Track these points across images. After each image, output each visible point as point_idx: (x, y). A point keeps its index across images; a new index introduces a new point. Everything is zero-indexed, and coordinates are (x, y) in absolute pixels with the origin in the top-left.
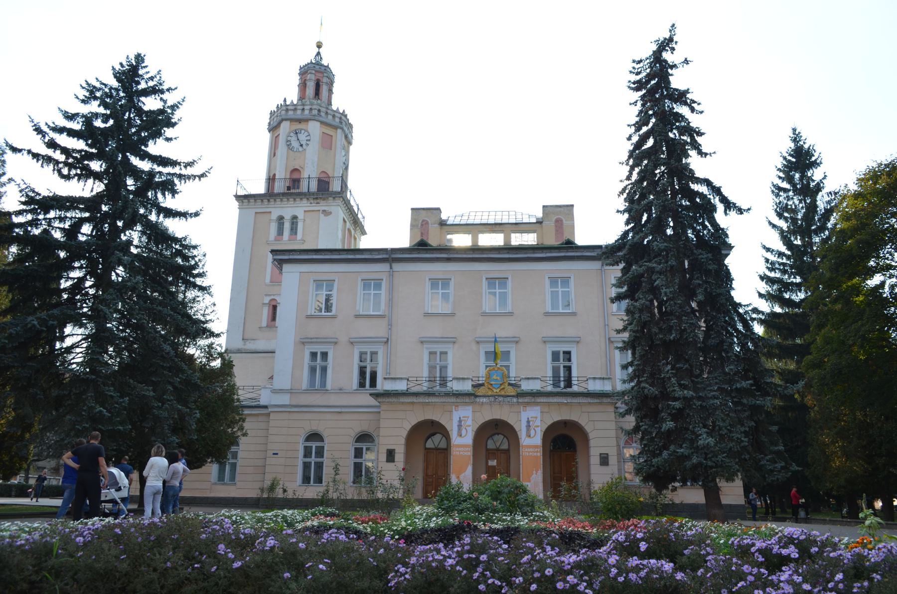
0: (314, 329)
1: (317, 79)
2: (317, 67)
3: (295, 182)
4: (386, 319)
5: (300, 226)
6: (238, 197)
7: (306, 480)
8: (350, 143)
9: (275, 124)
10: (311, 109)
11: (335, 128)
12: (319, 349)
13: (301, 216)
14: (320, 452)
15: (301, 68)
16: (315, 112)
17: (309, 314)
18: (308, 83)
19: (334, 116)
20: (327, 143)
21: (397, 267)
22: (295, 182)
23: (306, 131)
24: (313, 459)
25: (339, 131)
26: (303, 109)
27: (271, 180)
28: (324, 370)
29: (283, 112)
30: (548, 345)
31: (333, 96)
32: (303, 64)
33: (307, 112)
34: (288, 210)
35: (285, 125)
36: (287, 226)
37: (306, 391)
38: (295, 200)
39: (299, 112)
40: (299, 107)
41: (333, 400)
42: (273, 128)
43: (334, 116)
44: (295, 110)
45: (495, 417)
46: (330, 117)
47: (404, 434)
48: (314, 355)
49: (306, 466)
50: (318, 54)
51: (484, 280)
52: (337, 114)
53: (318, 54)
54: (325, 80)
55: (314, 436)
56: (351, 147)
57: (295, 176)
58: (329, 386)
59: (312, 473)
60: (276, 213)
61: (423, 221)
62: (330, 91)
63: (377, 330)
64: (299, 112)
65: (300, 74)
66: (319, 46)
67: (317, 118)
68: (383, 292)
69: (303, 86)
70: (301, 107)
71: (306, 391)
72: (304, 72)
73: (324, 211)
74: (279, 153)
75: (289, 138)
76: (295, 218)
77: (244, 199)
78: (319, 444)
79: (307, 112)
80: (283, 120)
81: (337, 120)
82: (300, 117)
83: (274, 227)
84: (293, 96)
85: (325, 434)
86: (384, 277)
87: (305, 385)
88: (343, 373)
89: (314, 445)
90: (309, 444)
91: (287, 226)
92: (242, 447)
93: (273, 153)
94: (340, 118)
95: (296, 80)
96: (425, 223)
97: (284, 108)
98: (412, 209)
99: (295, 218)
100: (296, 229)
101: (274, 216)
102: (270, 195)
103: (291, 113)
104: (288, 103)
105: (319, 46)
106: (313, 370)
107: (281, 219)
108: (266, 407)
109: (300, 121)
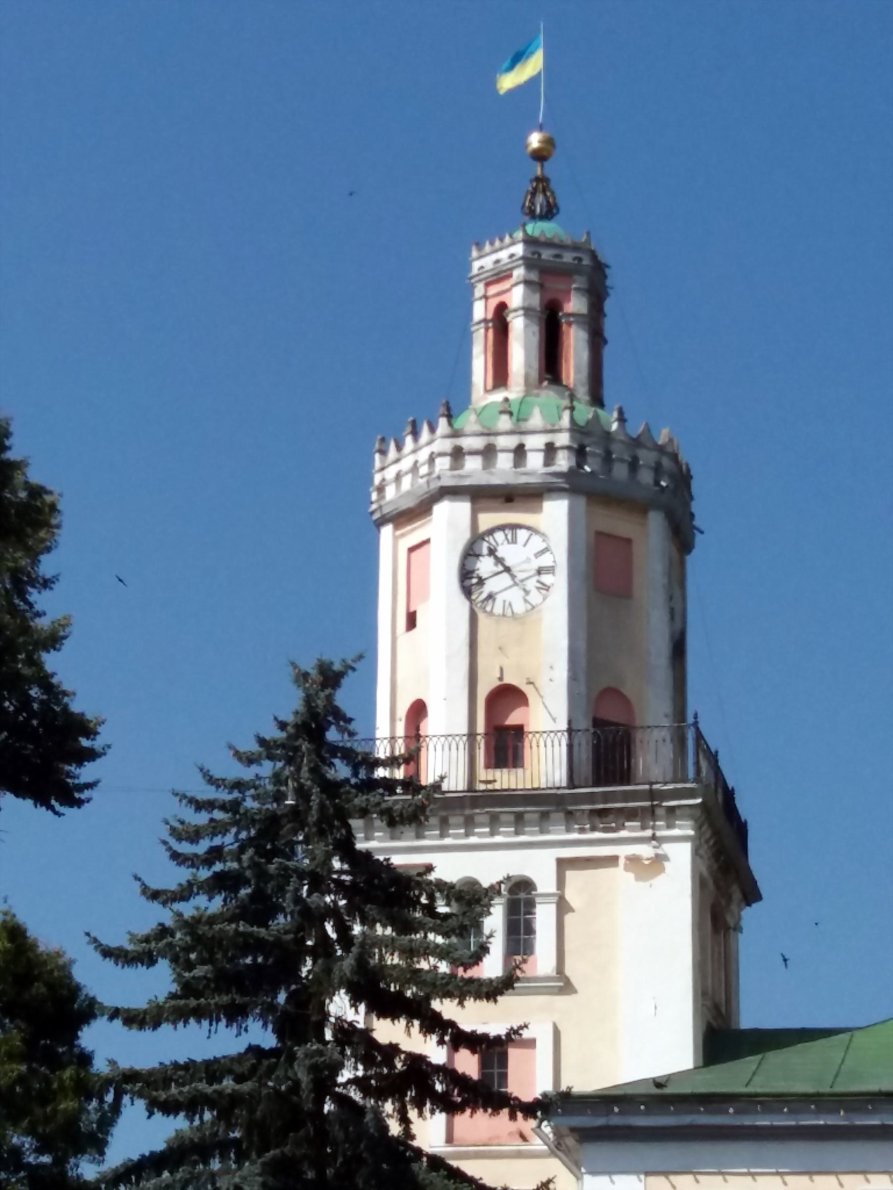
5: (544, 917)
9: (409, 503)
10: (550, 450)
11: (639, 508)
13: (545, 883)
19: (634, 465)
26: (520, 452)
29: (443, 464)
33: (535, 461)
39: (504, 461)
43: (634, 465)
46: (621, 471)
52: (646, 457)
54: (575, 304)
56: (689, 559)
64: (504, 461)
70: (511, 442)
73: (634, 861)
79: (535, 461)
81: (646, 476)
100: (530, 930)
103: (473, 464)
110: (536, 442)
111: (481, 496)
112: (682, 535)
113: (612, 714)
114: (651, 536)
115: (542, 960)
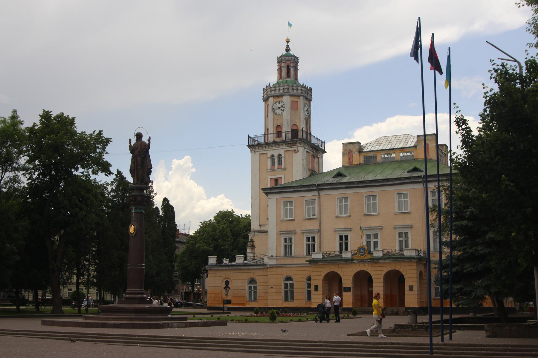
0: (284, 227)
1: (288, 64)
2: (287, 58)
3: (279, 134)
4: (318, 220)
5: (283, 159)
6: (249, 146)
7: (286, 299)
8: (310, 100)
11: (299, 96)
12: (288, 236)
13: (283, 155)
14: (292, 286)
15: (278, 58)
16: (286, 91)
17: (282, 219)
18: (282, 69)
20: (294, 107)
21: (322, 193)
22: (279, 134)
23: (282, 102)
24: (289, 289)
25: (301, 98)
26: (279, 90)
27: (266, 135)
28: (291, 246)
29: (269, 92)
30: (397, 230)
31: (299, 71)
32: (279, 56)
33: (281, 91)
34: (276, 151)
35: (271, 100)
36: (276, 160)
37: (283, 257)
38: (279, 145)
39: (277, 91)
40: (277, 88)
41: (296, 261)
42: (266, 100)
43: (297, 90)
44: (275, 90)
45: (355, 272)
47: (322, 278)
48: (285, 240)
49: (286, 292)
50: (288, 46)
51: (364, 197)
52: (299, 88)
53: (288, 46)
54: (292, 65)
55: (289, 279)
57: (279, 130)
58: (293, 254)
59: (289, 296)
60: (270, 153)
61: (350, 150)
62: (296, 70)
63: (314, 225)
64: (277, 91)
65: (278, 62)
66: (288, 41)
67: (287, 94)
68: (316, 206)
69: (280, 70)
71: (283, 257)
72: (280, 60)
73: (295, 150)
74: (269, 116)
75: (274, 107)
76: (280, 155)
77: (254, 146)
78: (291, 282)
79: (281, 91)
80: (270, 94)
81: (299, 91)
82: (279, 94)
83: (269, 162)
84: (273, 79)
85: (293, 278)
86: (316, 198)
87: (282, 254)
88: (299, 248)
89: (289, 282)
90: (287, 282)
91: (276, 160)
92: (258, 284)
93: (267, 116)
94: (302, 90)
95: (276, 66)
96: (350, 152)
97: (269, 90)
98: (343, 144)
99: (280, 155)
101: (269, 155)
102: (267, 144)
103: (273, 92)
104: (271, 86)
105: (288, 41)
106: (286, 247)
107: (273, 156)
108: (266, 265)
109: (278, 96)
110: (282, 88)
111: (274, 97)
112: (309, 99)
113: (295, 128)
114: (301, 101)
115: (283, 166)
